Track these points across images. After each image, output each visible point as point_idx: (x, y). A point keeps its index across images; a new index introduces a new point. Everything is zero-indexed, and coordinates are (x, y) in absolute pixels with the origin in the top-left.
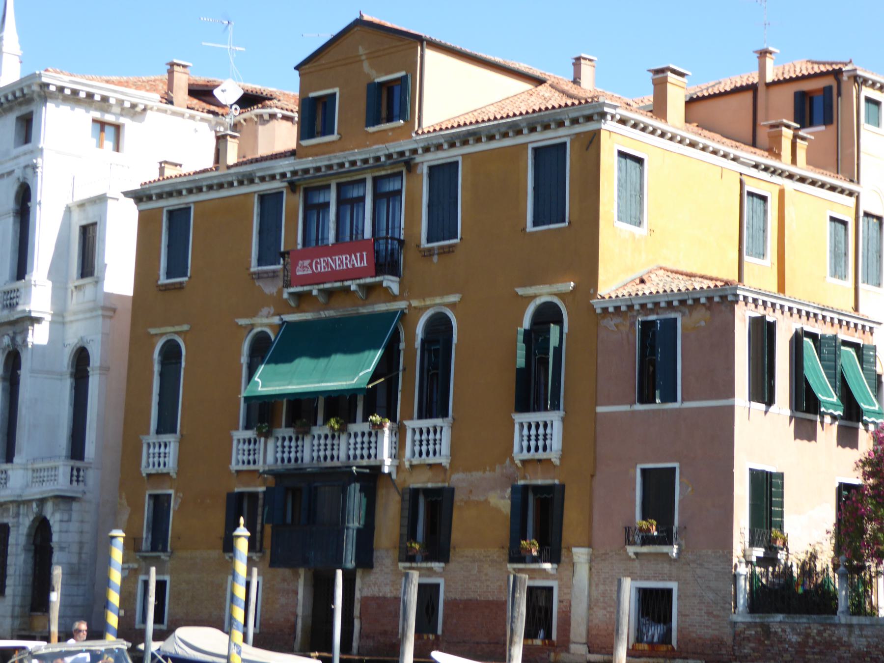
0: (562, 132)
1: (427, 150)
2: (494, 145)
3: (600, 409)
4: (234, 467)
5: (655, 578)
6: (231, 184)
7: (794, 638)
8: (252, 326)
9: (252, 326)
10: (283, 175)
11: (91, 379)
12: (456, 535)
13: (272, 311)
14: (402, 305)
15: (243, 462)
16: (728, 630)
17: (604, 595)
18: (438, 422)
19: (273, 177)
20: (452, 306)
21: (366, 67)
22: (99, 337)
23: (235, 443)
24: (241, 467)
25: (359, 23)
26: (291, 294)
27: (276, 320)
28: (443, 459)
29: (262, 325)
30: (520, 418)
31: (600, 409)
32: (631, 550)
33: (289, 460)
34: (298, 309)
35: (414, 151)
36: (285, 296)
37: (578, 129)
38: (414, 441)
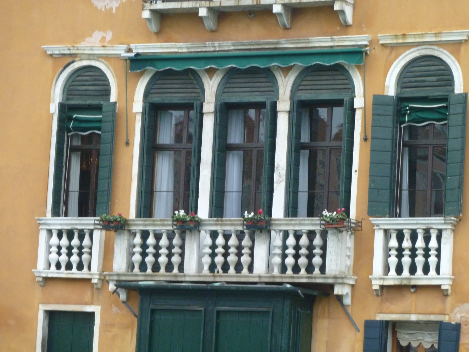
4: (41, 269)
8: (73, 57)
9: (73, 57)
13: (109, 36)
15: (58, 266)
18: (435, 222)
20: (455, 46)
23: (43, 235)
24: (53, 272)
26: (154, 12)
28: (444, 279)
29: (91, 57)
34: (160, 34)
36: (146, 14)
38: (387, 250)
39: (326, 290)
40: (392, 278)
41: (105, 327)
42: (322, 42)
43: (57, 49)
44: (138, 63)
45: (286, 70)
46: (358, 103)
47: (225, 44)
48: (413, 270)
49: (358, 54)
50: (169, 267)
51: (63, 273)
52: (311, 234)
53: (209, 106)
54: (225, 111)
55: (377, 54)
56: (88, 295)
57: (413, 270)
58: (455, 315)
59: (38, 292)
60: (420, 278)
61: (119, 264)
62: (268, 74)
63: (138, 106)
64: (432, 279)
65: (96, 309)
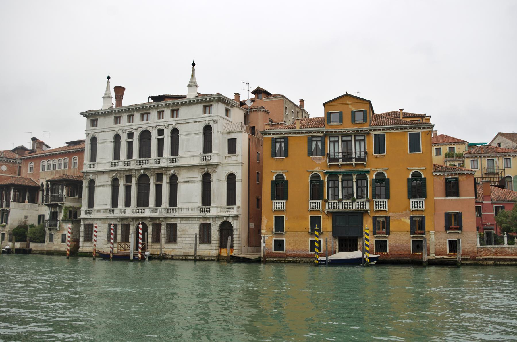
0: (419, 130)
1: (374, 130)
2: (397, 131)
3: (435, 198)
5: (454, 238)
6: (302, 133)
7: (494, 251)
8: (313, 172)
9: (313, 172)
10: (322, 132)
11: (237, 183)
12: (391, 228)
14: (368, 169)
16: (476, 249)
17: (439, 242)
19: (319, 132)
21: (350, 106)
22: (240, 171)
25: (347, 95)
27: (322, 171)
30: (411, 200)
31: (435, 198)
32: (448, 232)
33: (347, 208)
35: (371, 130)
37: (424, 130)
39: (367, 212)
40: (377, 209)
41: (323, 219)
42: (362, 170)
43: (310, 170)
44: (326, 173)
45: (354, 174)
46: (368, 180)
47: (344, 169)
48: (381, 208)
49: (368, 172)
50: (336, 208)
51: (314, 210)
52: (363, 202)
53: (340, 180)
54: (342, 181)
55: (371, 172)
56: (319, 213)
57: (381, 208)
58: (389, 215)
59: (309, 213)
60: (382, 209)
61: (327, 208)
62: (351, 175)
63: (326, 180)
64: (385, 209)
65: (321, 216)
